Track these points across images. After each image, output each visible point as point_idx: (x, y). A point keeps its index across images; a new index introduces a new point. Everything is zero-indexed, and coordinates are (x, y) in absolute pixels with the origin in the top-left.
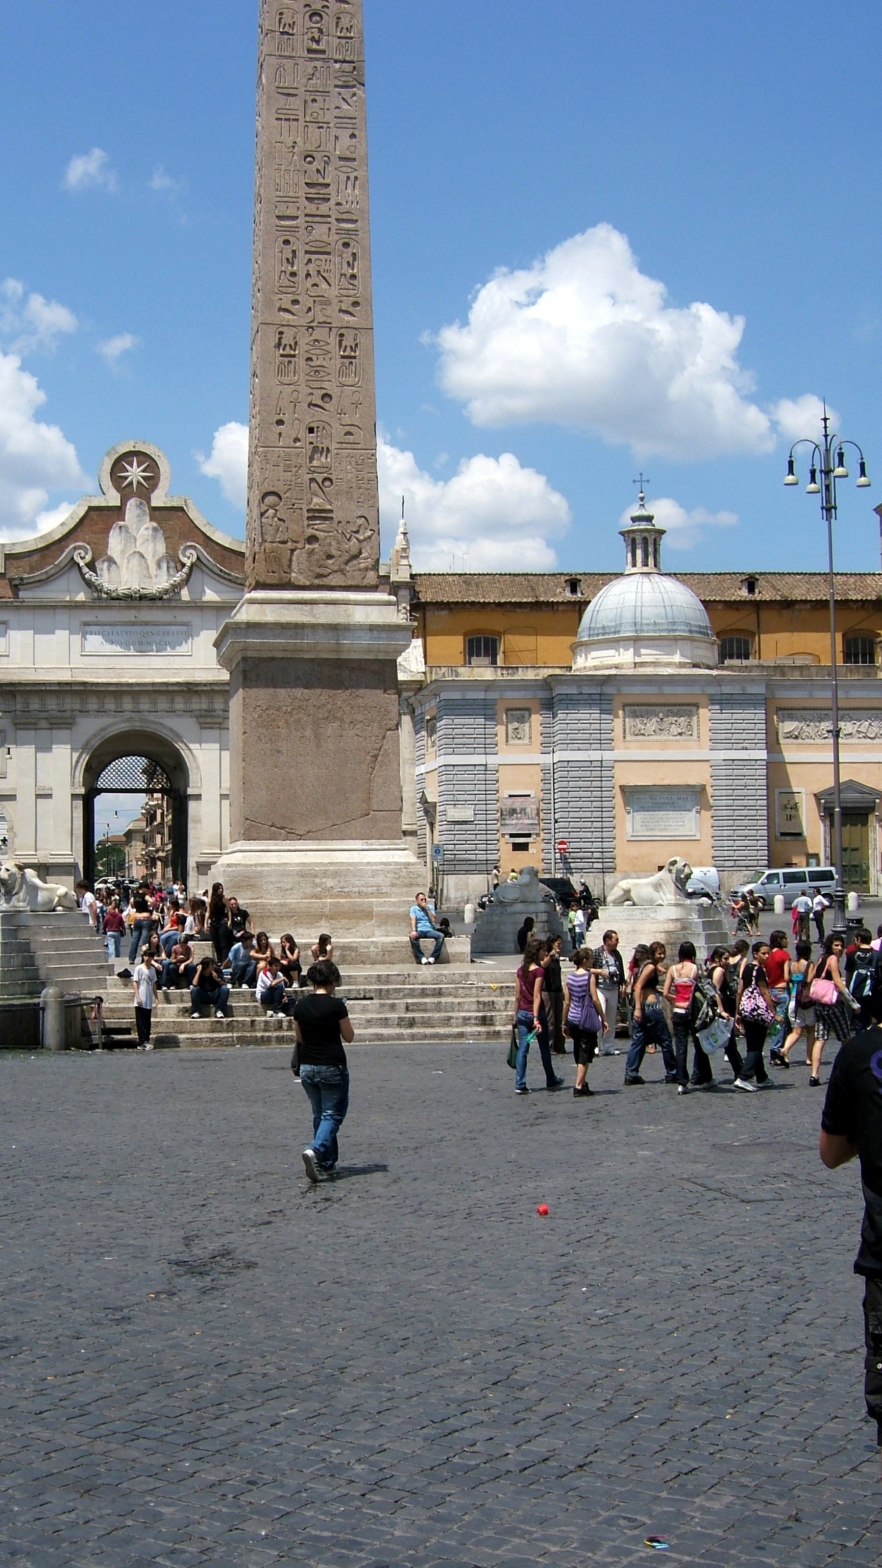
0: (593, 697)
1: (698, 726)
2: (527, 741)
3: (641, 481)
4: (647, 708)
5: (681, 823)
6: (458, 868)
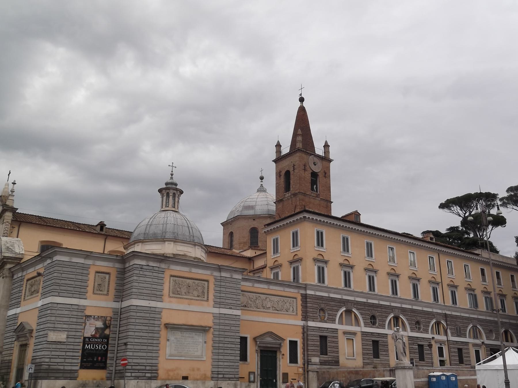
0: (155, 268)
1: (208, 293)
2: (105, 293)
3: (172, 166)
4: (182, 279)
5: (196, 350)
6: (50, 375)
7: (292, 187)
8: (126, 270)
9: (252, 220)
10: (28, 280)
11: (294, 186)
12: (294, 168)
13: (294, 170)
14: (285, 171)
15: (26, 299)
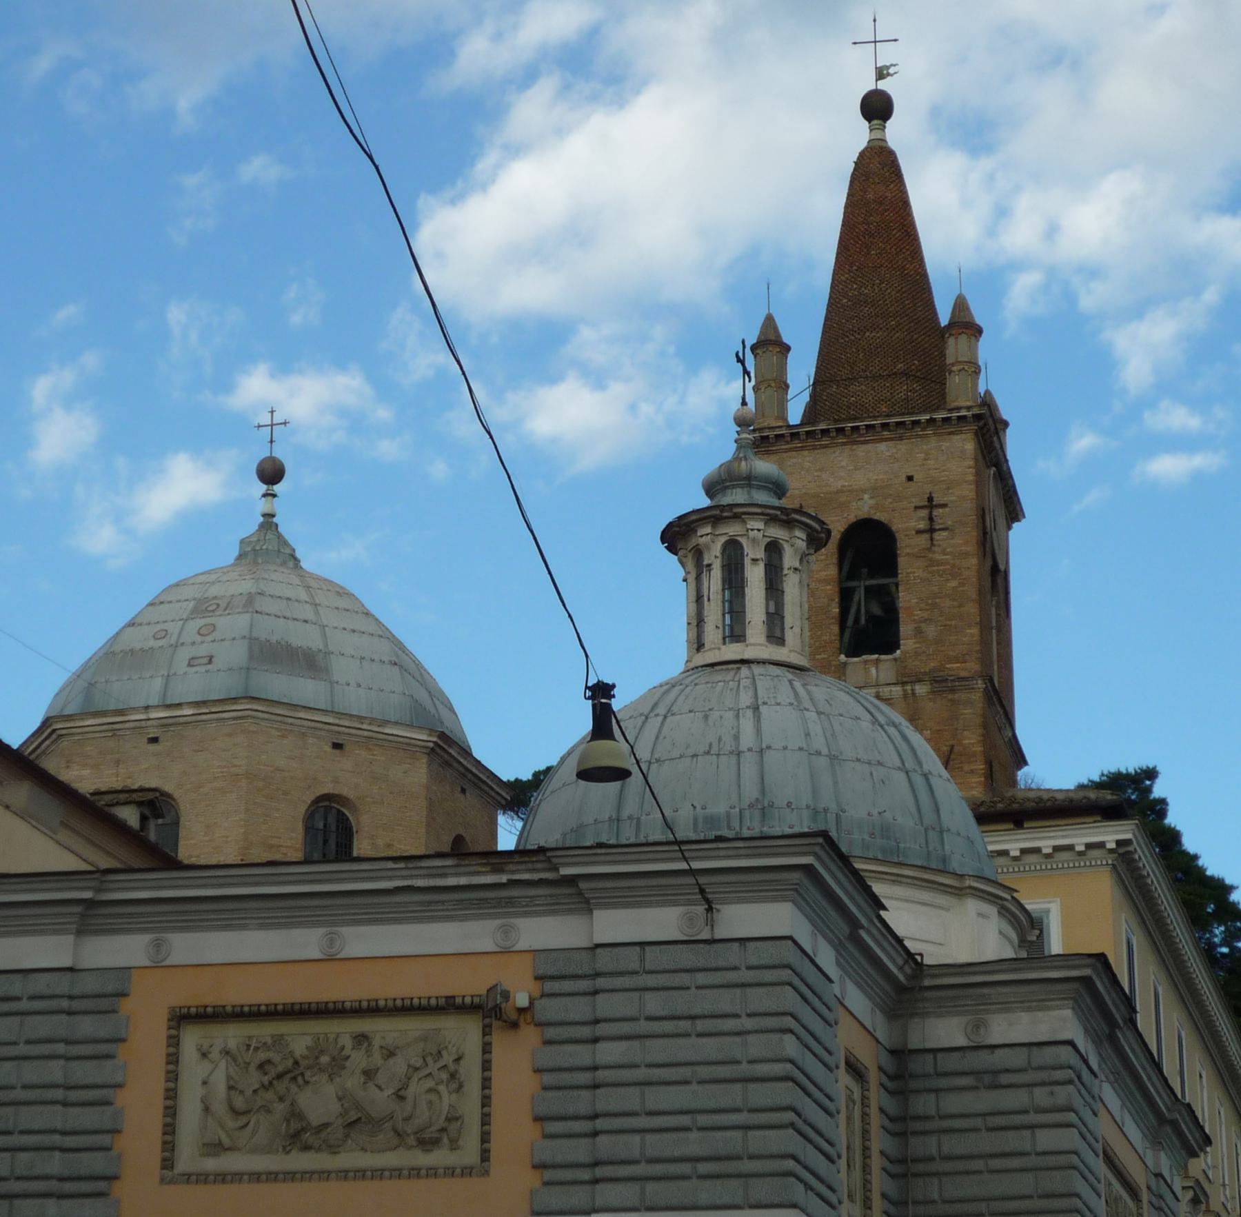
7: (919, 632)
8: (924, 1064)
9: (328, 748)
10: (182, 1018)
11: (931, 631)
12: (931, 519)
13: (931, 531)
14: (852, 519)
15: (182, 1165)
